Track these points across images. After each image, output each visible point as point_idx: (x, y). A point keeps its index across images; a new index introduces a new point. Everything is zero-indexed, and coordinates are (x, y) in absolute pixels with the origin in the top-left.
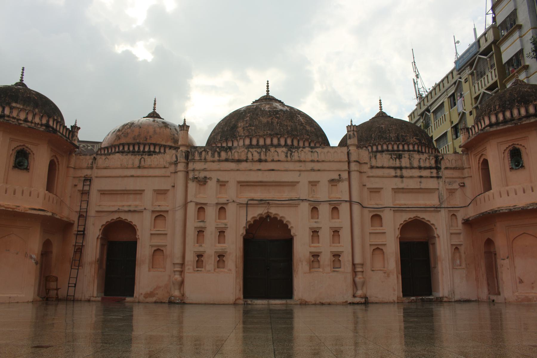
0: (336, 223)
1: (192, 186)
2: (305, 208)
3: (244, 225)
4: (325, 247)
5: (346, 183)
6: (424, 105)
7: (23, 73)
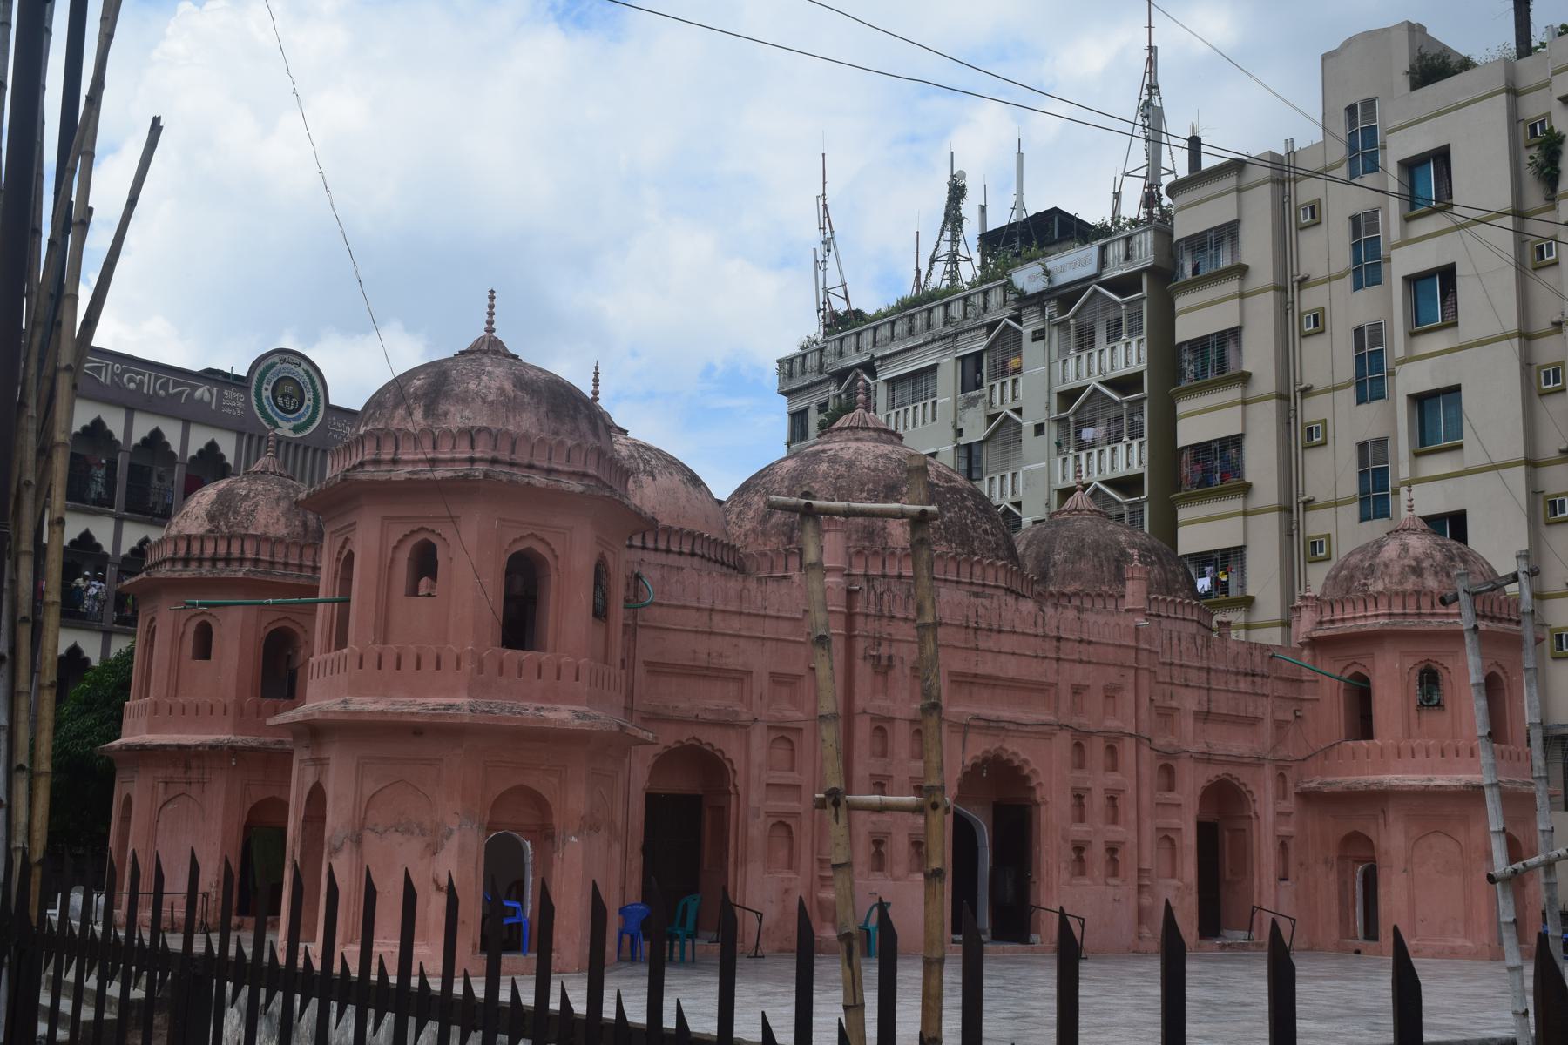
0: (1112, 779)
1: (863, 670)
2: (1063, 742)
3: (959, 775)
4: (1097, 831)
5: (1129, 695)
6: (858, 349)
7: (491, 307)
